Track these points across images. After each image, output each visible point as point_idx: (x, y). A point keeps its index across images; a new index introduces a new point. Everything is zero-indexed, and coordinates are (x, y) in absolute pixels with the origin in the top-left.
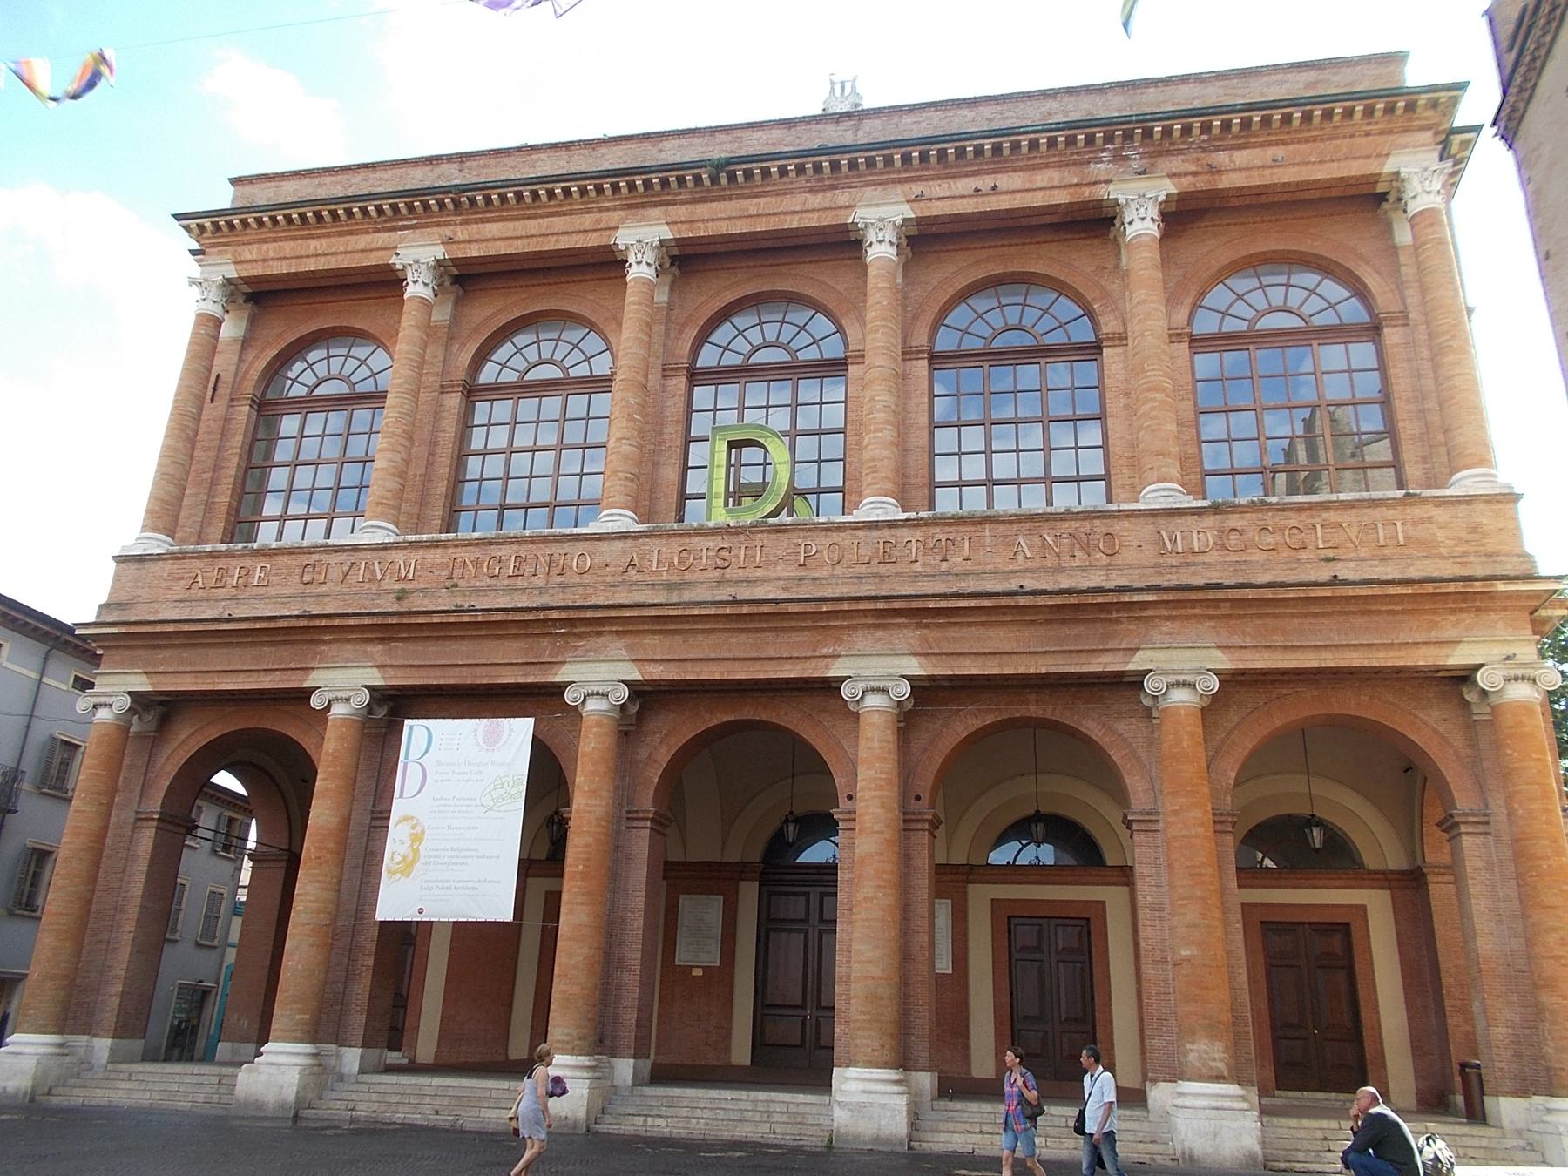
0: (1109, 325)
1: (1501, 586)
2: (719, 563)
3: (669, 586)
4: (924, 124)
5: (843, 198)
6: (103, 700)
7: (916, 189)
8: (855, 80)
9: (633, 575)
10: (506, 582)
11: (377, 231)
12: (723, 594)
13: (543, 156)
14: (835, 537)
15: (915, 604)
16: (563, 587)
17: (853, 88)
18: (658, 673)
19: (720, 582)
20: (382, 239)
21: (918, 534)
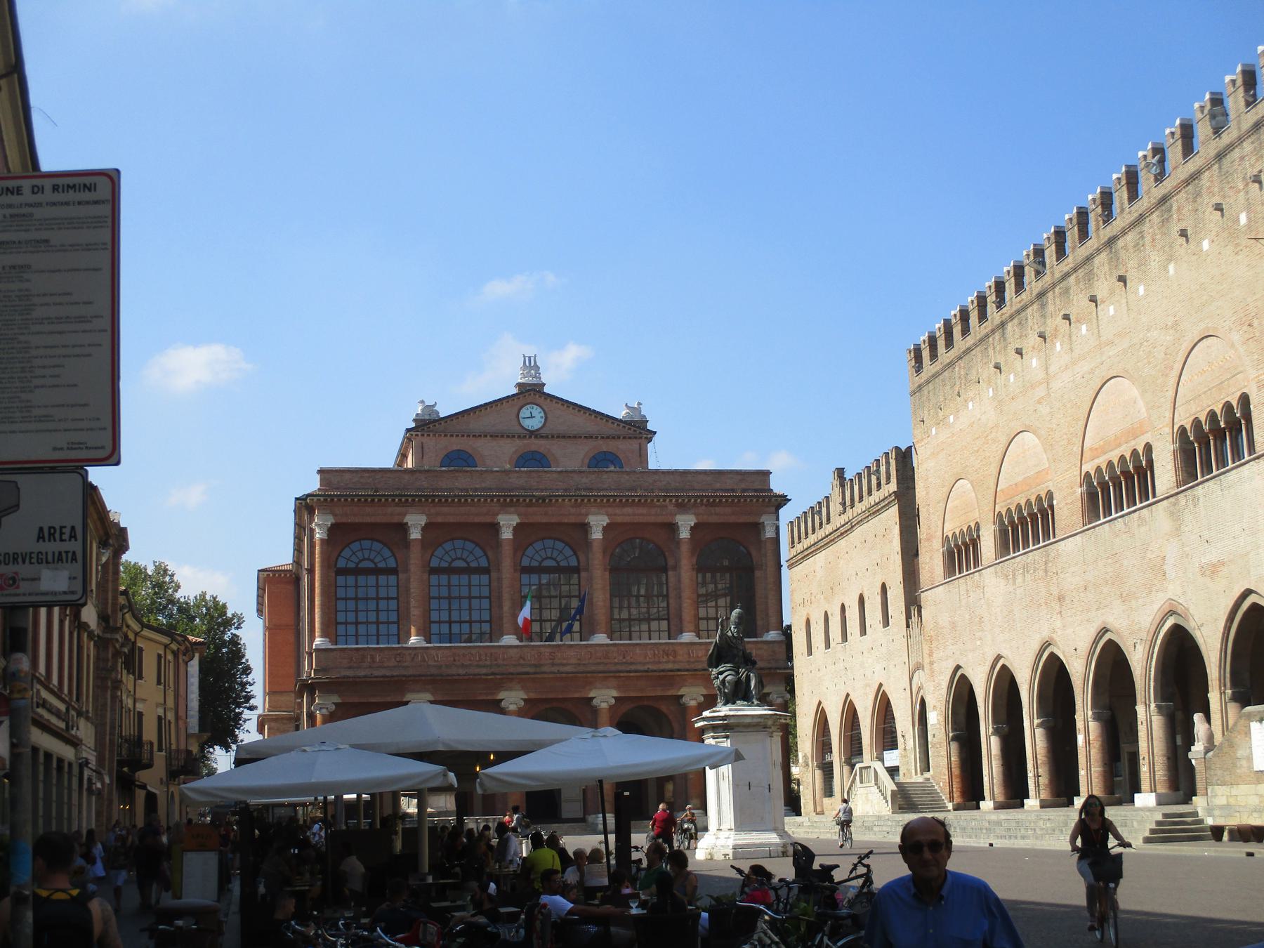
0: (671, 562)
1: (778, 671)
2: (551, 657)
3: (535, 666)
4: (610, 480)
5: (583, 511)
6: (324, 706)
7: (610, 510)
8: (535, 356)
9: (522, 662)
10: (476, 663)
11: (396, 506)
12: (555, 669)
13: (461, 474)
14: (589, 649)
15: (618, 674)
16: (498, 665)
17: (535, 362)
18: (533, 695)
19: (553, 665)
20: (399, 509)
21: (615, 649)
